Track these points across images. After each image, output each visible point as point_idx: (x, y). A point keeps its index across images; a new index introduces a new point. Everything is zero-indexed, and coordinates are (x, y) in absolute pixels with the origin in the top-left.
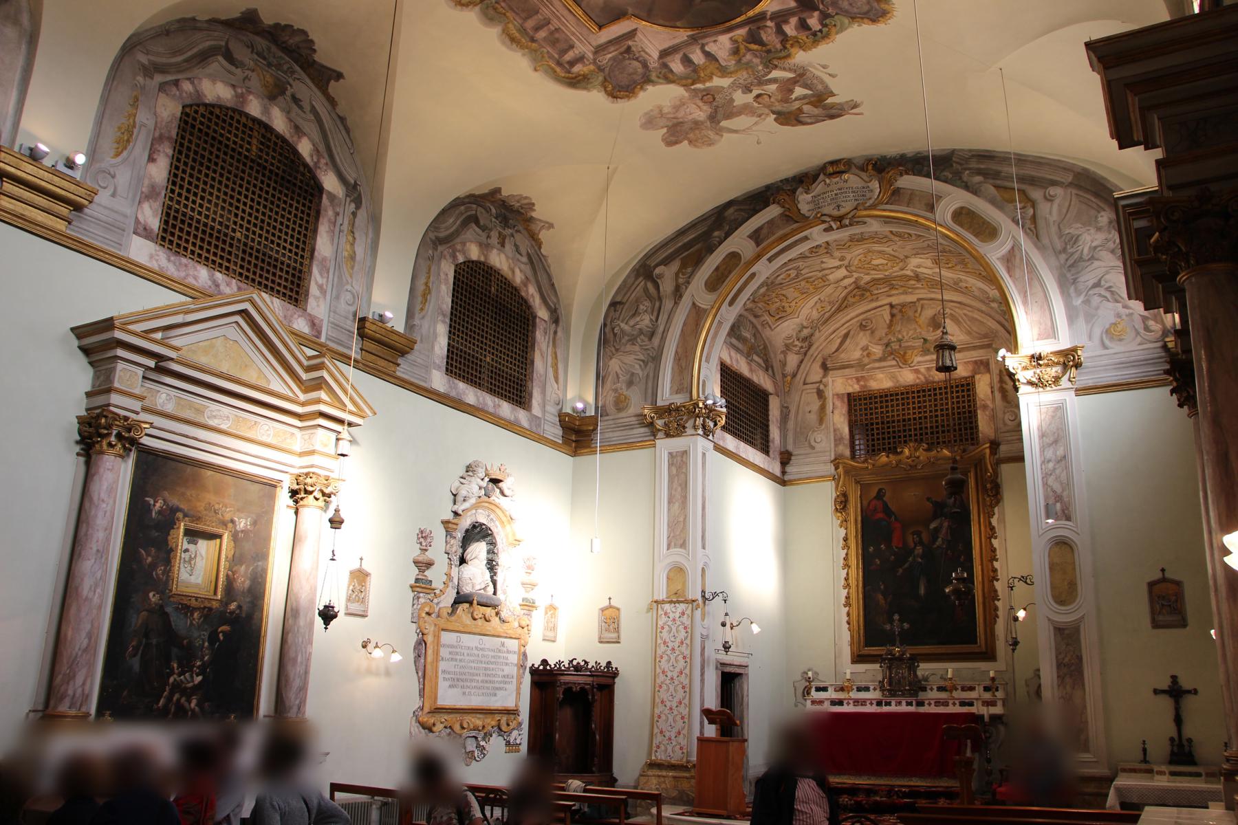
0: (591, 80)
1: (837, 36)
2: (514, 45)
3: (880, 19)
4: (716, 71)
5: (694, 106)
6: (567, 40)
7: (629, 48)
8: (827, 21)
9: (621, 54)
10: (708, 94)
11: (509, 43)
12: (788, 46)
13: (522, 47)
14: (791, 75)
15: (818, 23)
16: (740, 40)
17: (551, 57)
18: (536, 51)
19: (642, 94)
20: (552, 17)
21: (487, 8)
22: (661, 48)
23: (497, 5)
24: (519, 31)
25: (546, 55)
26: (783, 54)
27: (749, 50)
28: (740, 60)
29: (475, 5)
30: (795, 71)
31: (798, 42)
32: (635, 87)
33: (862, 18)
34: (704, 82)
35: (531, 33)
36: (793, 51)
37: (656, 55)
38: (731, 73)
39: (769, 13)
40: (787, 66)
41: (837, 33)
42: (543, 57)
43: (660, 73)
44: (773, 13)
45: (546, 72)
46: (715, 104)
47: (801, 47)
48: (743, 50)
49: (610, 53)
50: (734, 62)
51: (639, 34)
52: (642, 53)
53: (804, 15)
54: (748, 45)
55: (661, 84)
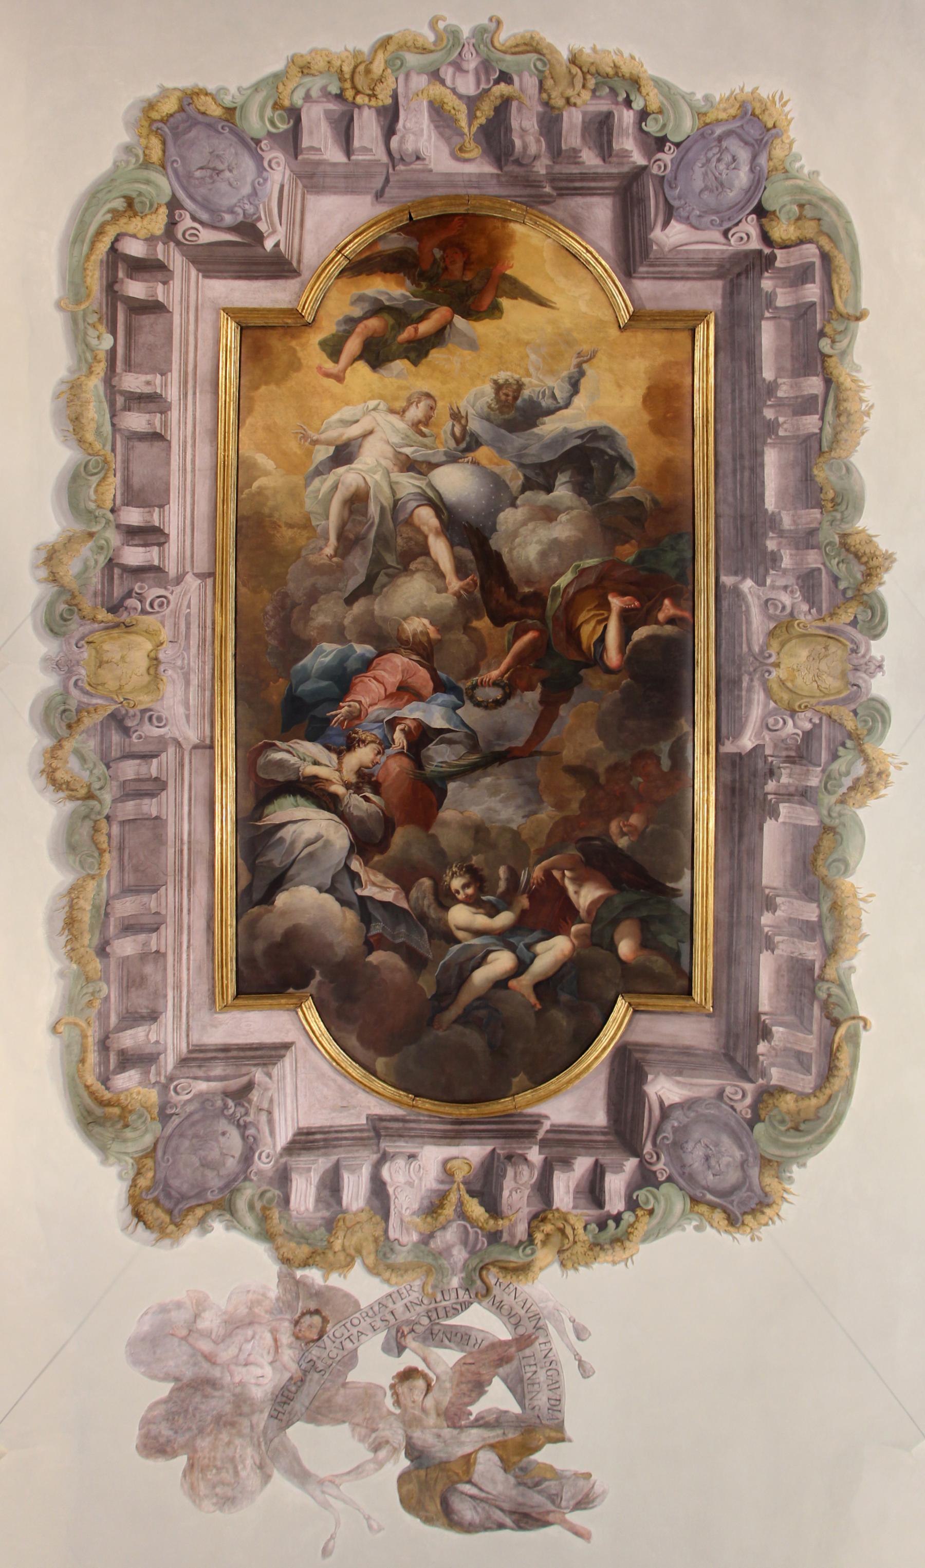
0: (129, 1133)
1: (643, 1247)
2: (63, 939)
3: (748, 1219)
4: (369, 1247)
5: (268, 1337)
6: (159, 995)
7: (249, 1087)
8: (642, 1195)
9: (226, 1094)
10: (317, 1312)
11: (60, 924)
12: (539, 1237)
13: (73, 954)
14: (502, 1332)
15: (623, 1193)
16: (459, 1177)
17: (103, 1016)
18: (88, 980)
19: (192, 1240)
20: (170, 920)
21: (86, 817)
22: (301, 1125)
23: (104, 824)
24: (96, 907)
25: (97, 1003)
26: (517, 1258)
27: (462, 1215)
28: (431, 1235)
29: (71, 798)
30: (516, 1325)
31: (562, 1231)
32: (191, 1209)
33: (713, 1206)
34: (329, 1268)
35: (112, 930)
36: (544, 1256)
37: (284, 1135)
38: (392, 1268)
39: (547, 1125)
40: (508, 1299)
41: (646, 1239)
42: (90, 1003)
43: (262, 1194)
44: (554, 1130)
45: (67, 1047)
46: (315, 1352)
47: (560, 1252)
48: (449, 1211)
49: (208, 1079)
50: (415, 1237)
51: (287, 1062)
52: (264, 1117)
53: (607, 1159)
54: (466, 1197)
55: (245, 1229)
